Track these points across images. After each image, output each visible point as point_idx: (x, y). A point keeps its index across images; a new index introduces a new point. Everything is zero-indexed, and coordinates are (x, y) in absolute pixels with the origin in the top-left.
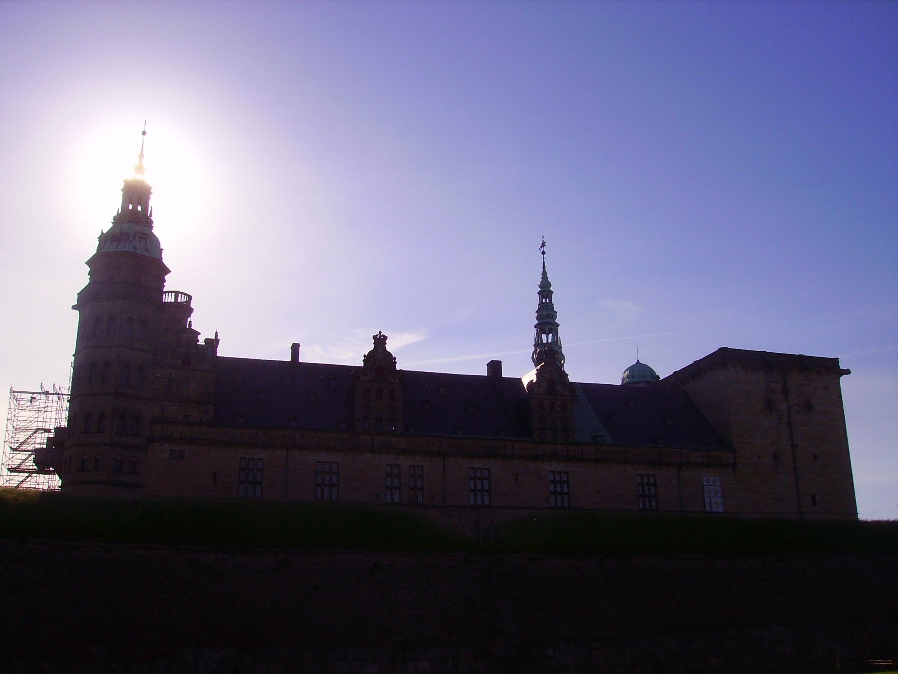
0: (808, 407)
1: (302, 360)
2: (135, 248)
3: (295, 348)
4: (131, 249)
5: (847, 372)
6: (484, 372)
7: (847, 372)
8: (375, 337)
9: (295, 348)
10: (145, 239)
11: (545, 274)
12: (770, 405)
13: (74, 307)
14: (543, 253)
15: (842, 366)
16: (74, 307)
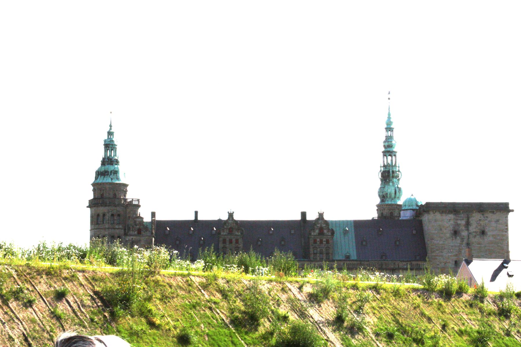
0: (483, 233)
1: (200, 218)
2: (112, 179)
3: (196, 213)
4: (110, 181)
5: (513, 211)
6: (299, 218)
7: (513, 211)
8: (228, 212)
9: (196, 213)
10: (116, 173)
11: (389, 114)
12: (456, 233)
13: (87, 207)
14: (389, 99)
15: (511, 208)
16: (87, 207)
